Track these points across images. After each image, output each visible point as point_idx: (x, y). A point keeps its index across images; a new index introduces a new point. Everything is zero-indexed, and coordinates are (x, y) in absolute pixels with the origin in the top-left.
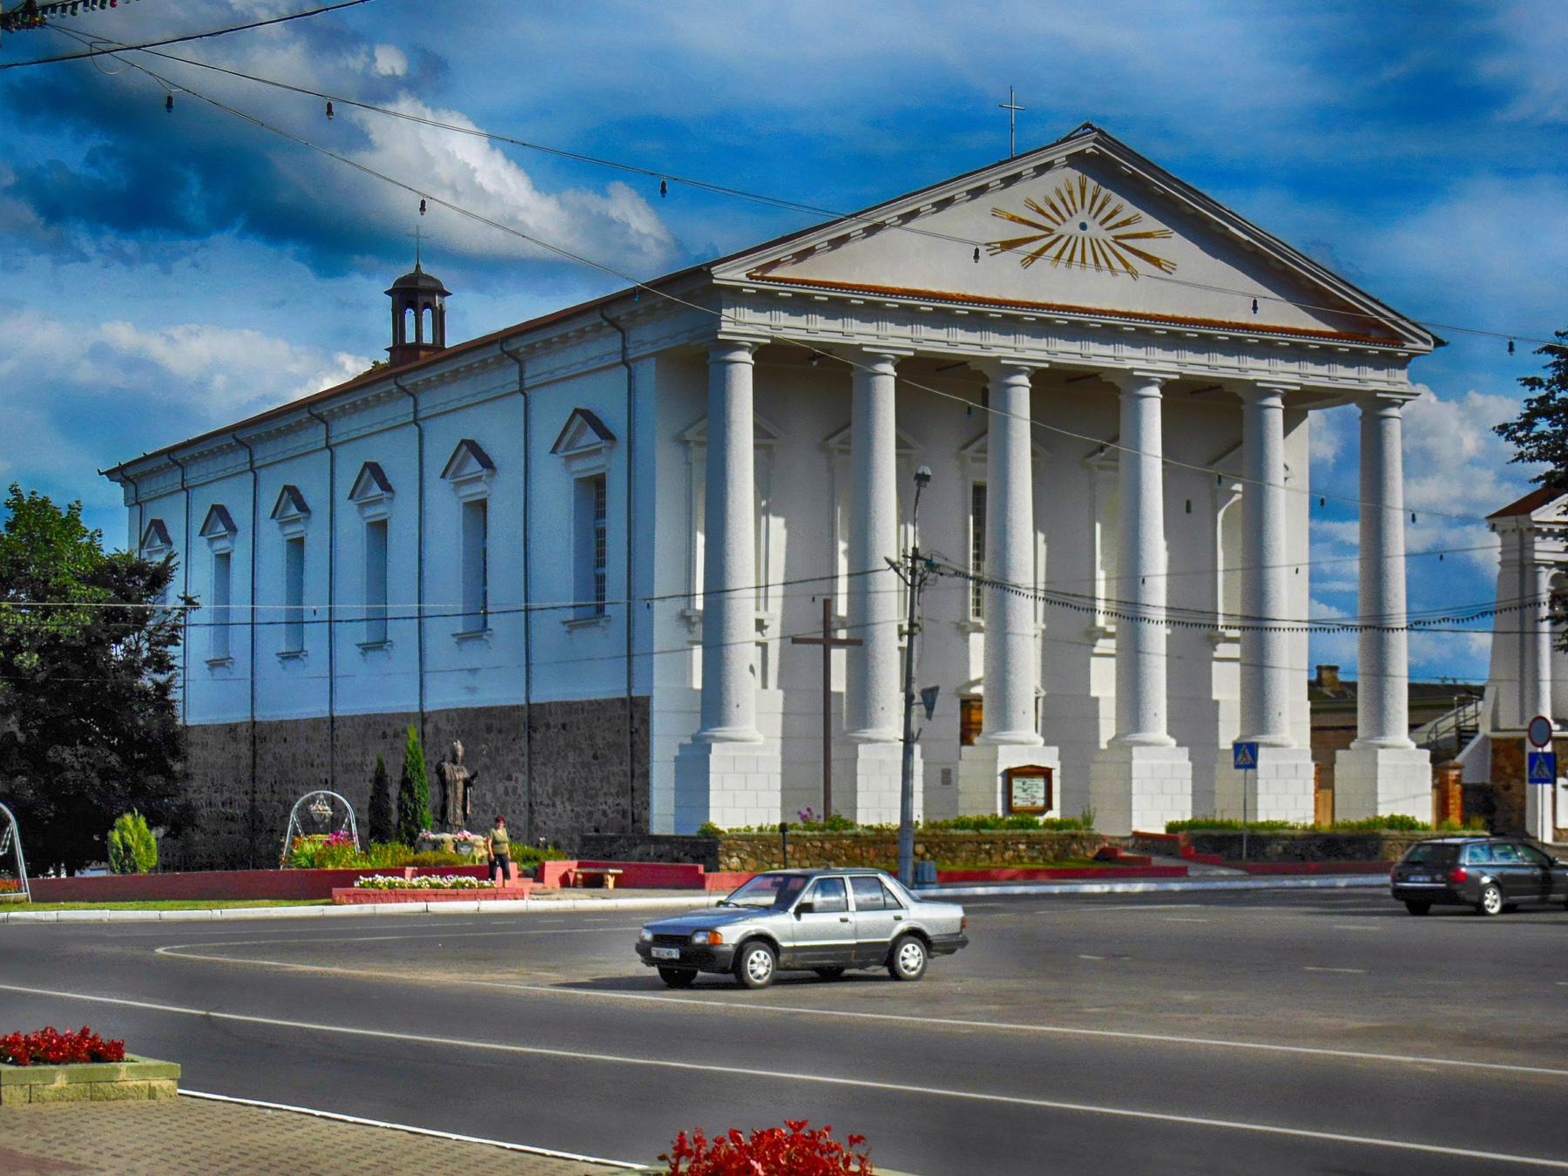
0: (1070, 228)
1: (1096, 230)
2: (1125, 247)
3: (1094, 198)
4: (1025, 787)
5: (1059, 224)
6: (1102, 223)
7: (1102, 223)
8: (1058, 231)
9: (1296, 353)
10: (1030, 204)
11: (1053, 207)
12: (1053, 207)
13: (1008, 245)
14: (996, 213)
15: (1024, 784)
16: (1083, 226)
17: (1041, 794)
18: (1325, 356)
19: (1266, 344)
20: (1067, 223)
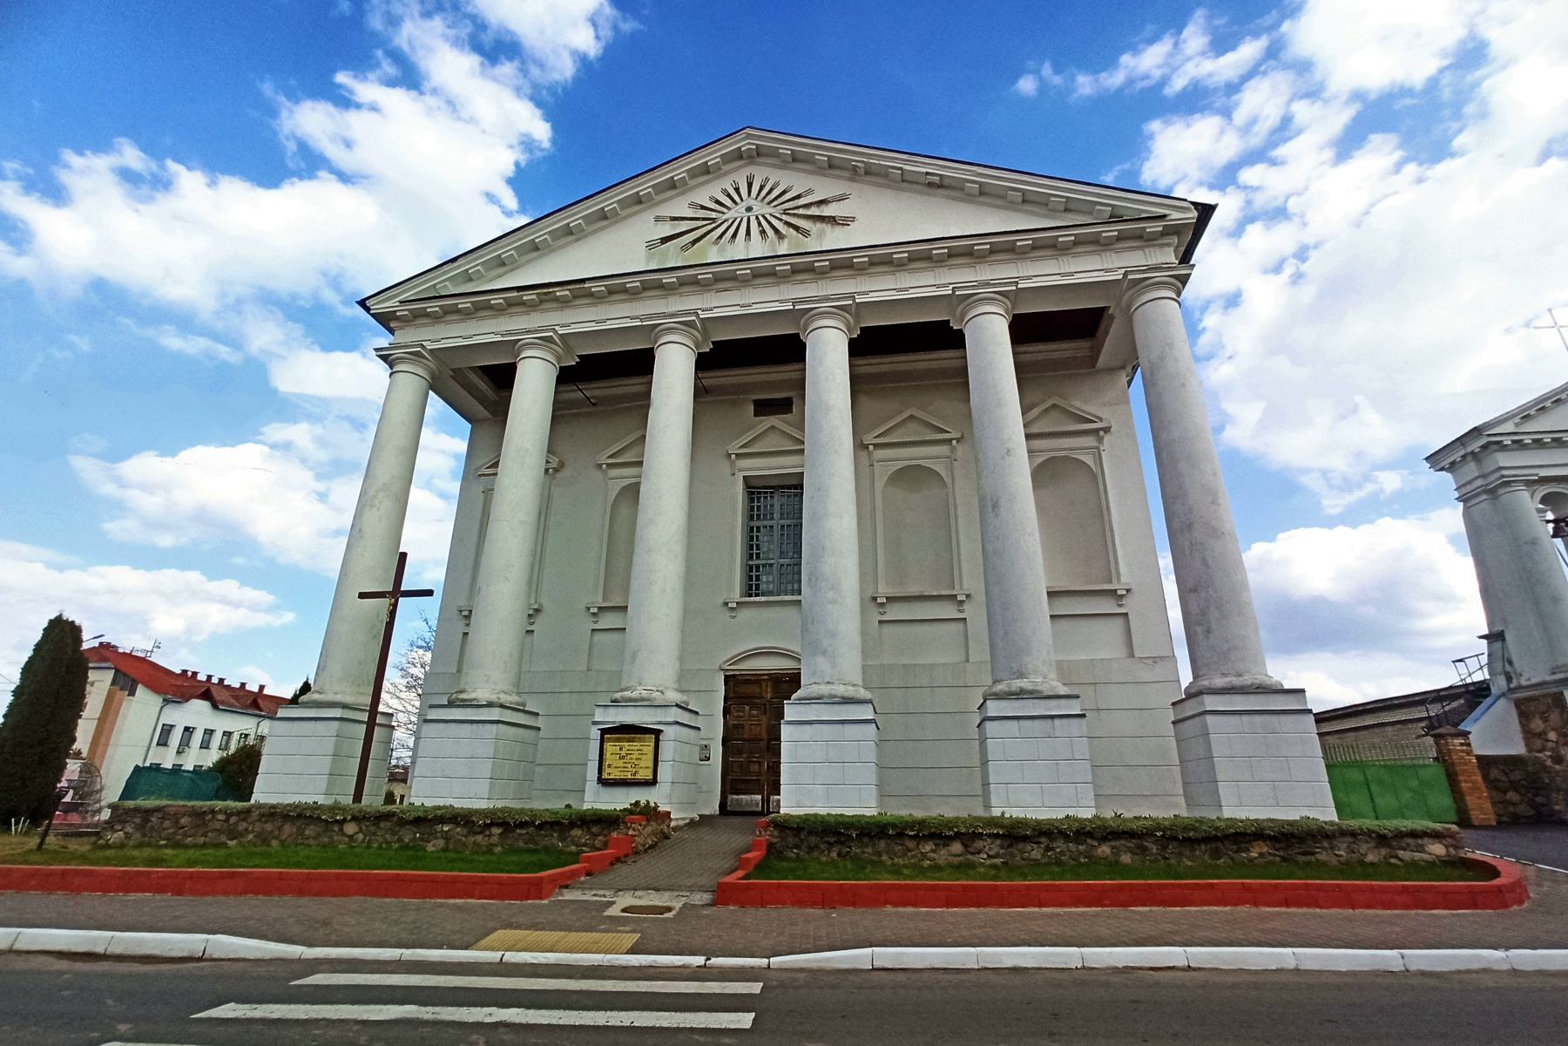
0: (738, 212)
1: (760, 209)
2: (795, 215)
3: (762, 188)
4: (623, 753)
5: (723, 213)
6: (769, 203)
7: (769, 203)
8: (725, 217)
9: (1003, 248)
10: (693, 205)
11: (718, 202)
12: (718, 202)
13: (665, 240)
14: (658, 219)
15: (621, 749)
16: (749, 209)
17: (648, 761)
18: (1045, 246)
19: (962, 251)
20: (731, 212)
